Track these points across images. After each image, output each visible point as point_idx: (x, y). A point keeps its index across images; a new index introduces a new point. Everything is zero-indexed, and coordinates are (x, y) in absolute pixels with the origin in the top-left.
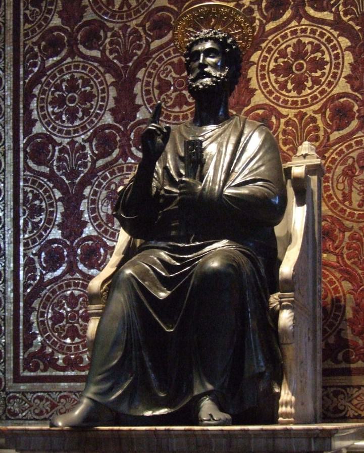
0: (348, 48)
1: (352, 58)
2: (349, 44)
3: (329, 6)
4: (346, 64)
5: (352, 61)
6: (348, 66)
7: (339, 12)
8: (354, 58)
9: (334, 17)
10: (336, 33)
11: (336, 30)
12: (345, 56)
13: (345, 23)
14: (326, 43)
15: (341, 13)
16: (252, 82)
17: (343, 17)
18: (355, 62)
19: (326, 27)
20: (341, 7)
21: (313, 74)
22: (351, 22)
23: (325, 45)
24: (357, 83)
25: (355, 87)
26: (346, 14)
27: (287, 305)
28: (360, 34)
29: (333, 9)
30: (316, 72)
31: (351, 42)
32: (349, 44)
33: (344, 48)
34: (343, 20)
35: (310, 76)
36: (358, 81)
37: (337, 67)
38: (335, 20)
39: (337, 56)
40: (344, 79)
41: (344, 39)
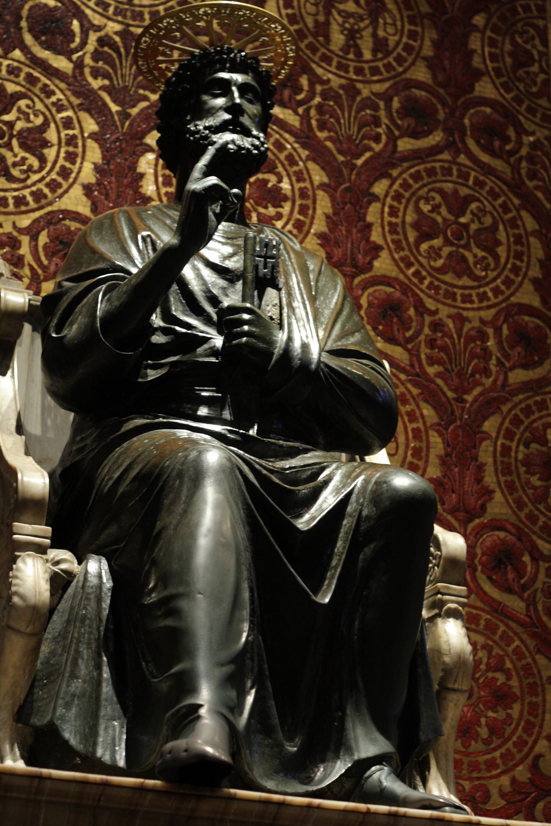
0: (322, 186)
1: (329, 205)
2: (326, 180)
3: (293, 101)
4: (319, 212)
5: (330, 211)
6: (323, 218)
7: (310, 118)
8: (333, 206)
9: (301, 124)
10: (304, 153)
11: (304, 146)
12: (318, 197)
13: (319, 142)
14: (286, 163)
15: (314, 123)
16: (144, 183)
17: (316, 130)
18: (335, 214)
19: (287, 136)
20: (313, 112)
21: (262, 210)
22: (329, 144)
23: (283, 165)
24: (338, 253)
25: (335, 259)
26: (322, 126)
27: (456, 610)
28: (344, 169)
29: (300, 110)
30: (266, 207)
31: (330, 178)
32: (326, 180)
33: (316, 183)
34: (316, 136)
35: (256, 210)
36: (340, 250)
37: (303, 210)
38: (301, 130)
39: (303, 194)
40: (315, 238)
41: (317, 167)
